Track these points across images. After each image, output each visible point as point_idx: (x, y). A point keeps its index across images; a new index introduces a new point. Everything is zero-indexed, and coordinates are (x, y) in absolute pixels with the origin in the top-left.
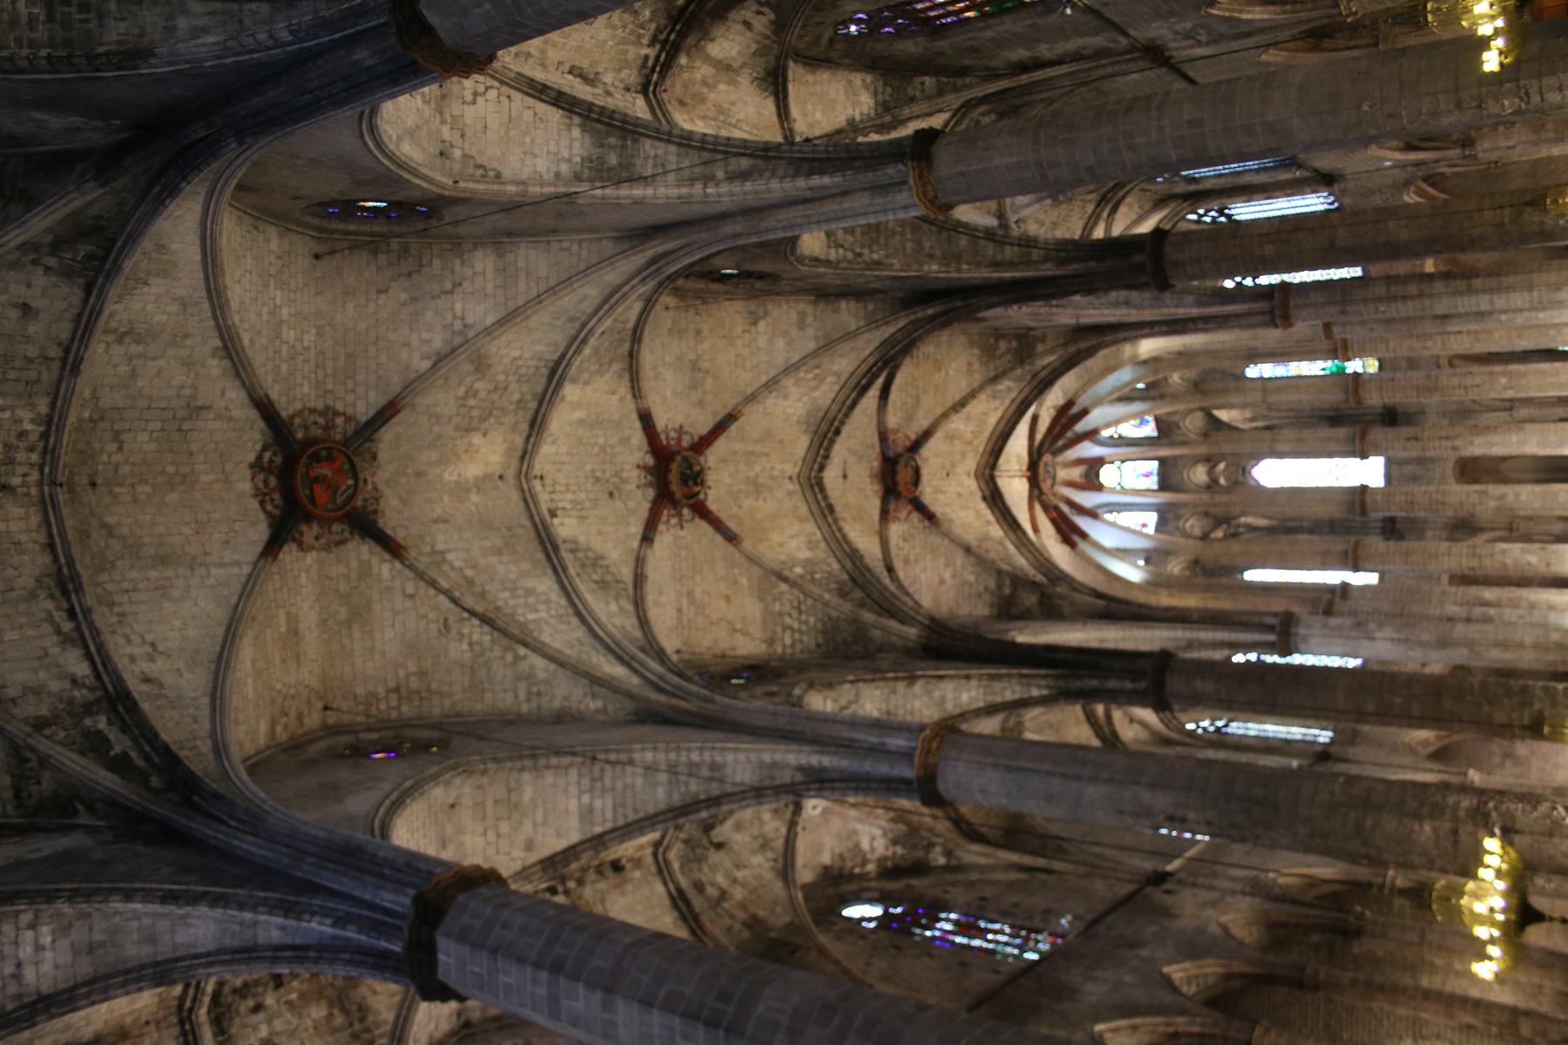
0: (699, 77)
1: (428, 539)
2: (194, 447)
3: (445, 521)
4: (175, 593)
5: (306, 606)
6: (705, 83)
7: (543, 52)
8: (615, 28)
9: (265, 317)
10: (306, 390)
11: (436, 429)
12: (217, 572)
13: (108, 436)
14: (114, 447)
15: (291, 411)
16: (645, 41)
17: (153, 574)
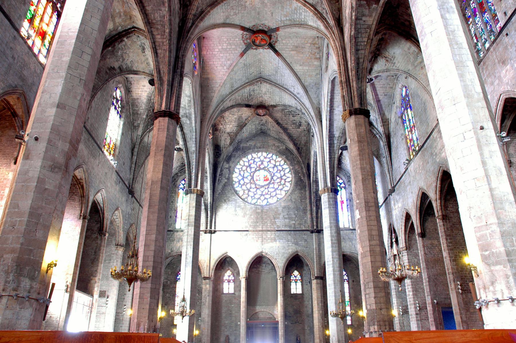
0: (120, 20)
1: (277, 20)
2: (252, 61)
3: (272, 13)
4: (283, 75)
5: (291, 42)
6: (120, 16)
7: (144, 61)
8: (128, 55)
9: (222, 55)
10: (237, 39)
11: (245, 15)
12: (280, 65)
13: (251, 76)
14: (253, 74)
15: (243, 44)
16: (124, 43)
17: (279, 75)
